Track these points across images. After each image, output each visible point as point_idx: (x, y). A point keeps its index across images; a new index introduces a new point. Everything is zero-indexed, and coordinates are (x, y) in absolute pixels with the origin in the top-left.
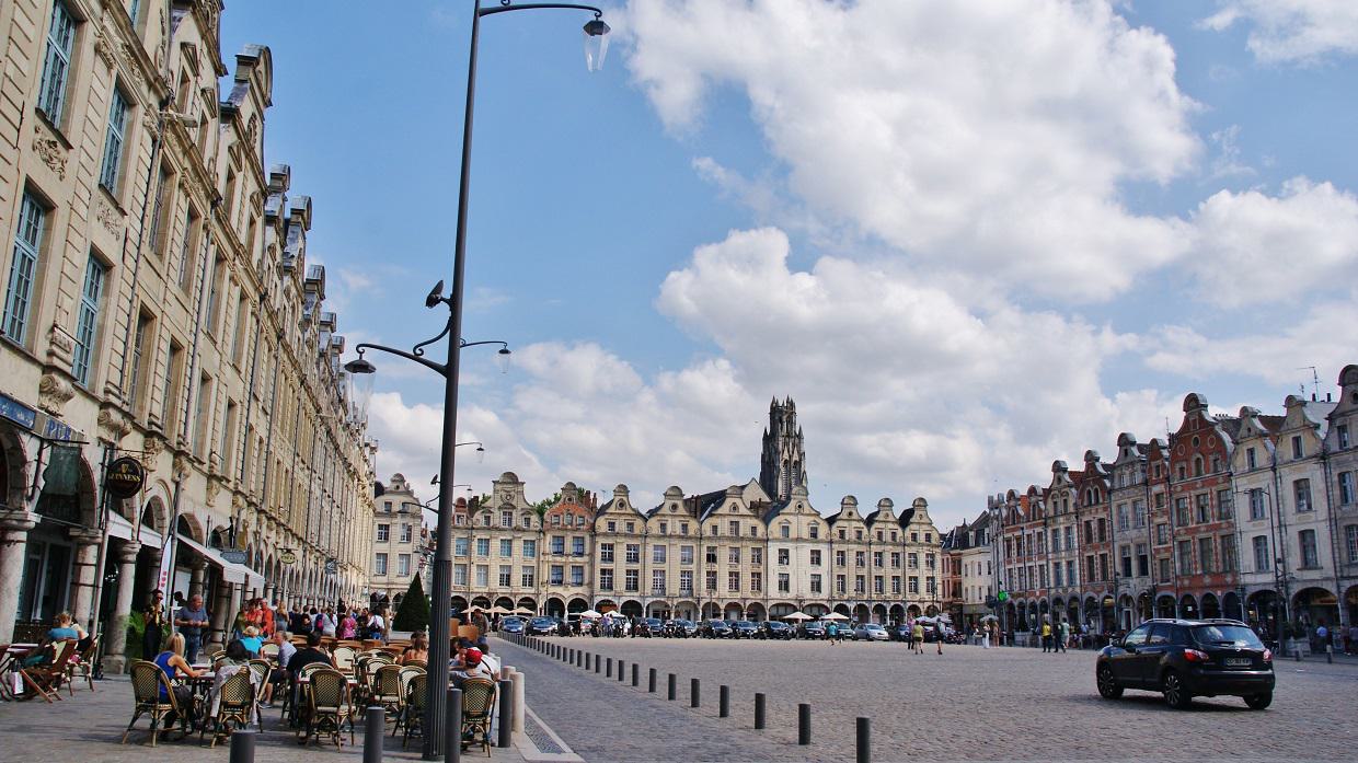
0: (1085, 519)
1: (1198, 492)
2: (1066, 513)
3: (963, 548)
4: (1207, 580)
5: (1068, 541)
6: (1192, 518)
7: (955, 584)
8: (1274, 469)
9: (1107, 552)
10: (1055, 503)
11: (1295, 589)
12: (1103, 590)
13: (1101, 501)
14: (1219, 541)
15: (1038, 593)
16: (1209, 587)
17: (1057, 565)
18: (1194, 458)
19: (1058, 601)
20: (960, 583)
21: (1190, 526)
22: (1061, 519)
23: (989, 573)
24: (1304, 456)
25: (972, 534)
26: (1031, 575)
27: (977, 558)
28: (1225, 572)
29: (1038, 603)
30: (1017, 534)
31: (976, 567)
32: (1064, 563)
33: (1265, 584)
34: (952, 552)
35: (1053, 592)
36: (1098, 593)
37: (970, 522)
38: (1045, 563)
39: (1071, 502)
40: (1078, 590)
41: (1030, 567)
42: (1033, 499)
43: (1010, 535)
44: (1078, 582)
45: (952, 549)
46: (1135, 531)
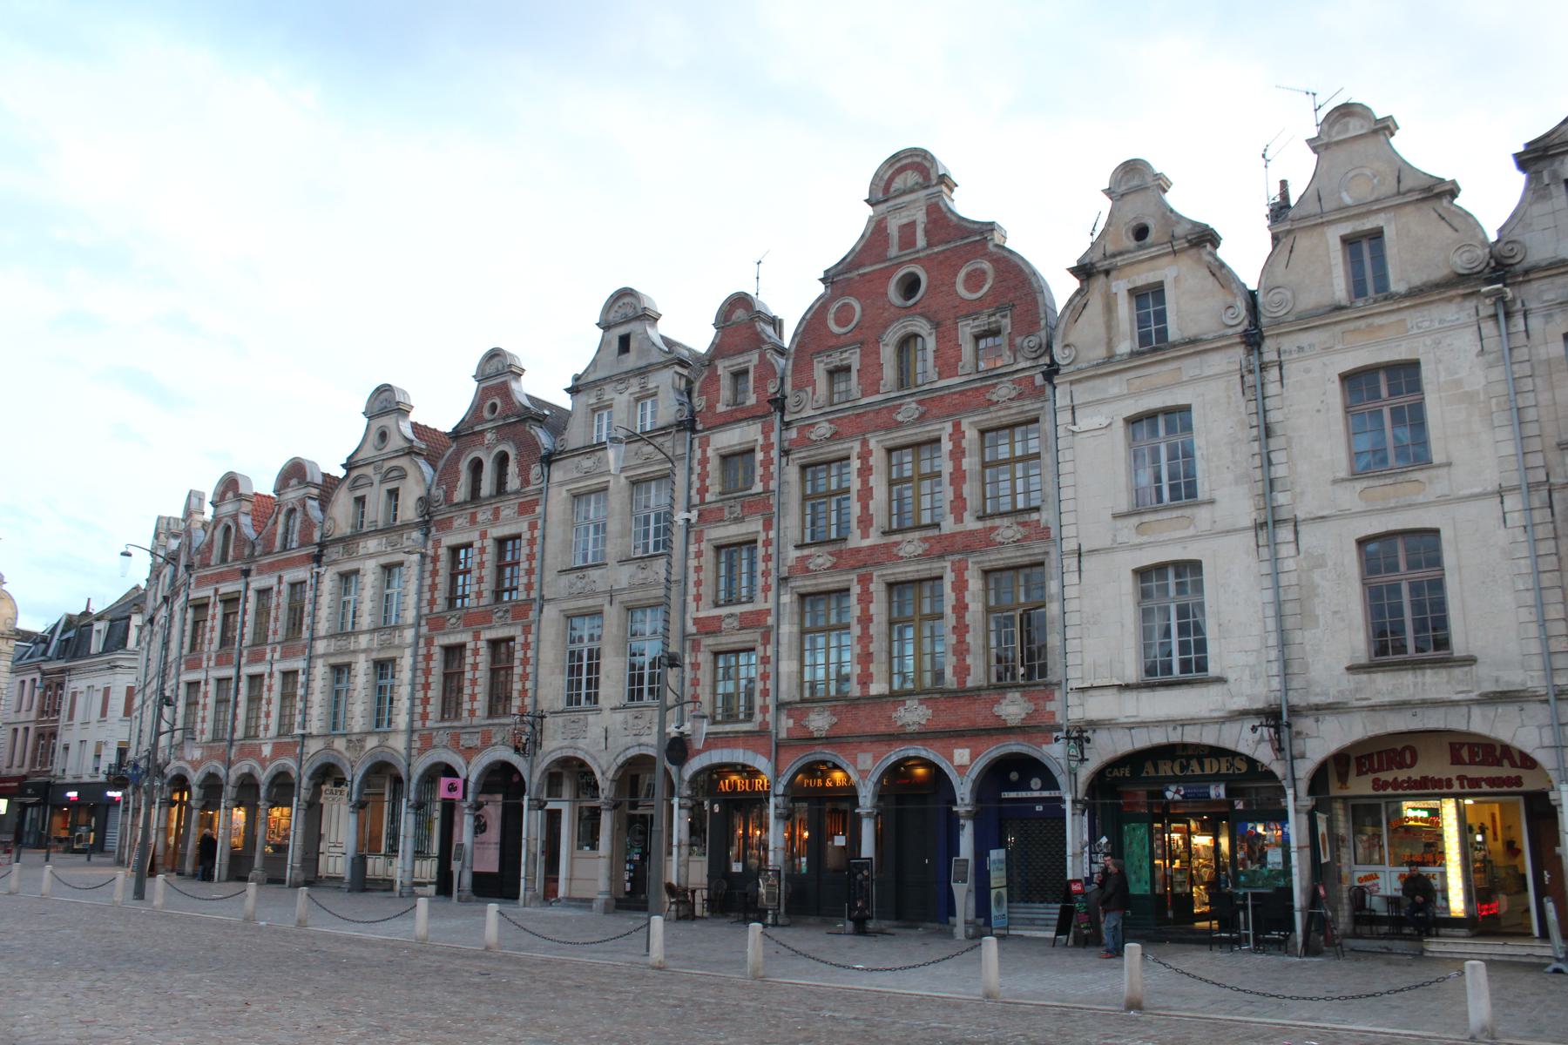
0: (450, 540)
1: (898, 437)
2: (391, 529)
3: (74, 657)
4: (913, 714)
5: (385, 602)
6: (865, 521)
7: (40, 736)
8: (1253, 339)
9: (515, 631)
10: (360, 501)
11: (1323, 740)
12: (487, 743)
13: (513, 482)
14: (975, 584)
15: (267, 750)
16: (922, 736)
17: (340, 671)
18: (893, 335)
19: (328, 773)
20: (54, 735)
21: (856, 541)
22: (372, 545)
23: (128, 711)
24: (1396, 285)
25: (98, 626)
26: (255, 699)
27: (100, 681)
28: (1001, 686)
29: (263, 777)
30: (227, 588)
31: (98, 699)
32: (362, 667)
33: (1183, 723)
34: (45, 667)
35: (314, 746)
36: (469, 753)
37: (96, 608)
38: (299, 664)
39: (411, 493)
40: (399, 743)
41: (255, 679)
42: (292, 495)
43: (208, 592)
44: (402, 721)
45: (50, 659)
46: (629, 569)
